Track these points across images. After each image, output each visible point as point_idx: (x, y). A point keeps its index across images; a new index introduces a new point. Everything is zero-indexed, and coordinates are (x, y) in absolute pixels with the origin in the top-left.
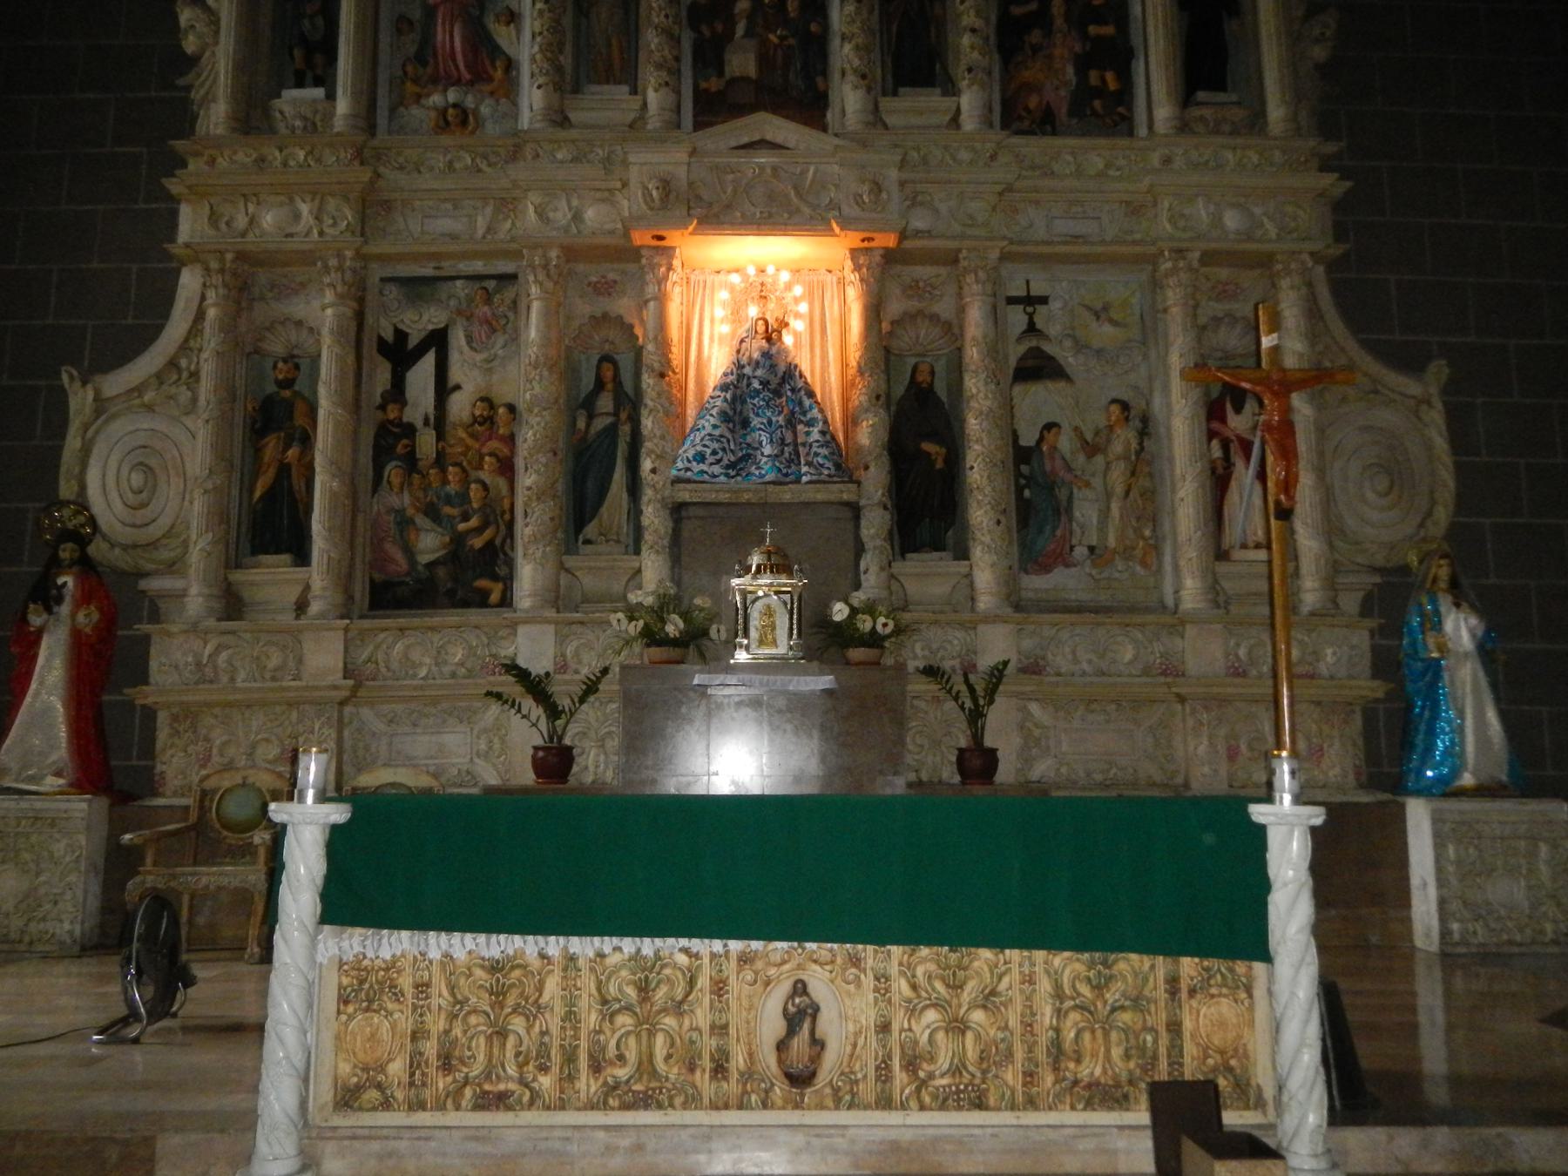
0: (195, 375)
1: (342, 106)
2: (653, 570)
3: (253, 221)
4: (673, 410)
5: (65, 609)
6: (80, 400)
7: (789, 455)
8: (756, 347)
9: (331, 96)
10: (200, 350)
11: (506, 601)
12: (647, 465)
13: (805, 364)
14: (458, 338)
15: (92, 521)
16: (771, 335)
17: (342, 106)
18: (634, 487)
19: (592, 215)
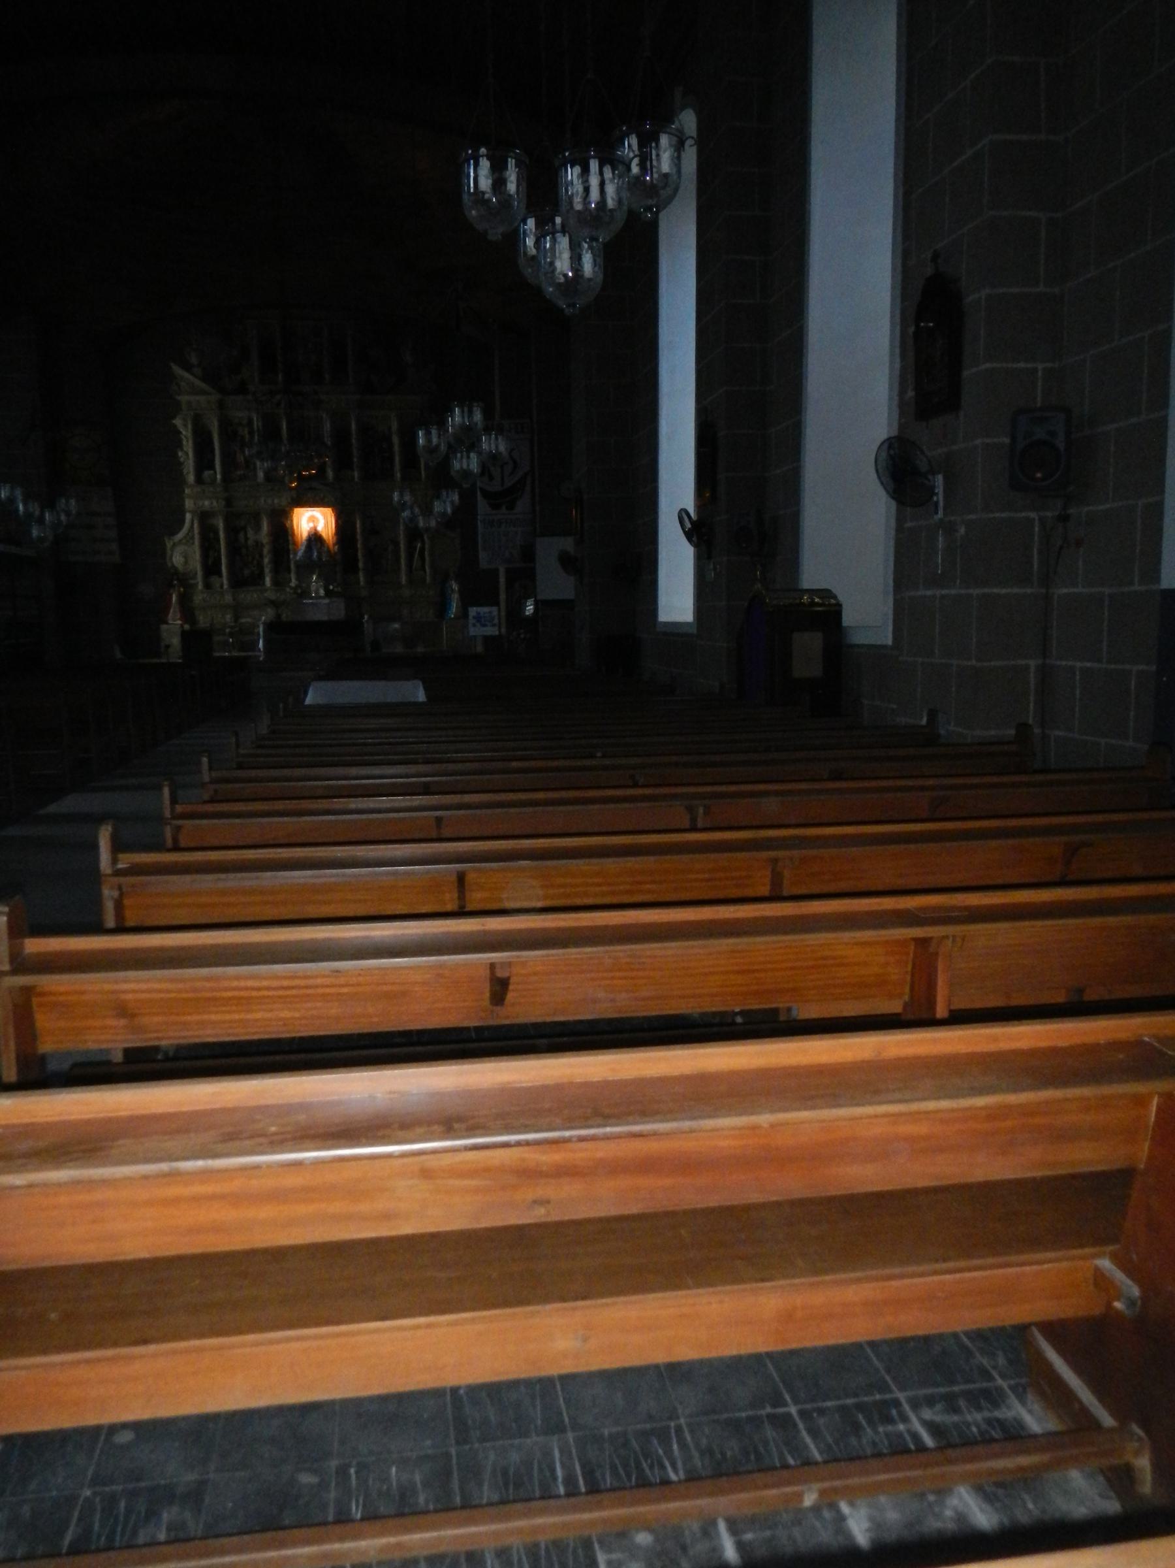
0: (193, 538)
1: (219, 477)
2: (293, 576)
3: (203, 504)
4: (295, 544)
5: (176, 588)
6: (169, 544)
7: (320, 554)
8: (313, 531)
9: (216, 473)
10: (193, 531)
11: (264, 584)
12: (291, 556)
13: (324, 535)
14: (249, 529)
15: (176, 569)
16: (316, 530)
17: (219, 477)
18: (289, 560)
19: (276, 501)
